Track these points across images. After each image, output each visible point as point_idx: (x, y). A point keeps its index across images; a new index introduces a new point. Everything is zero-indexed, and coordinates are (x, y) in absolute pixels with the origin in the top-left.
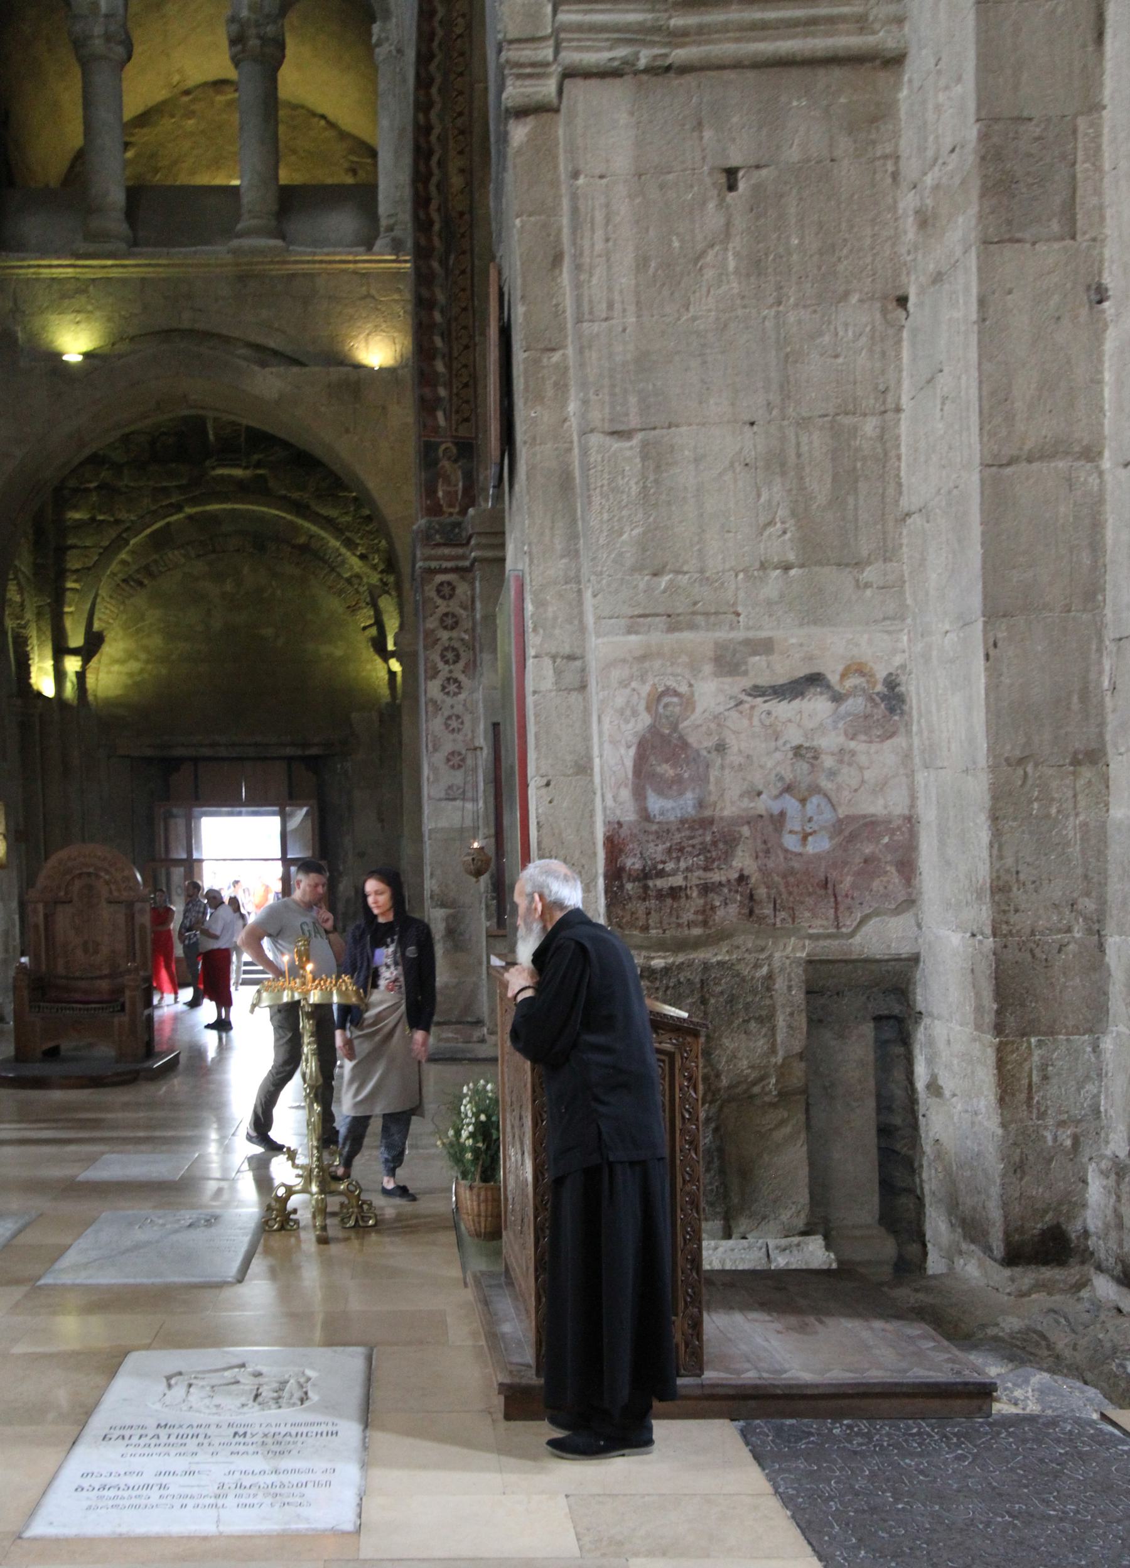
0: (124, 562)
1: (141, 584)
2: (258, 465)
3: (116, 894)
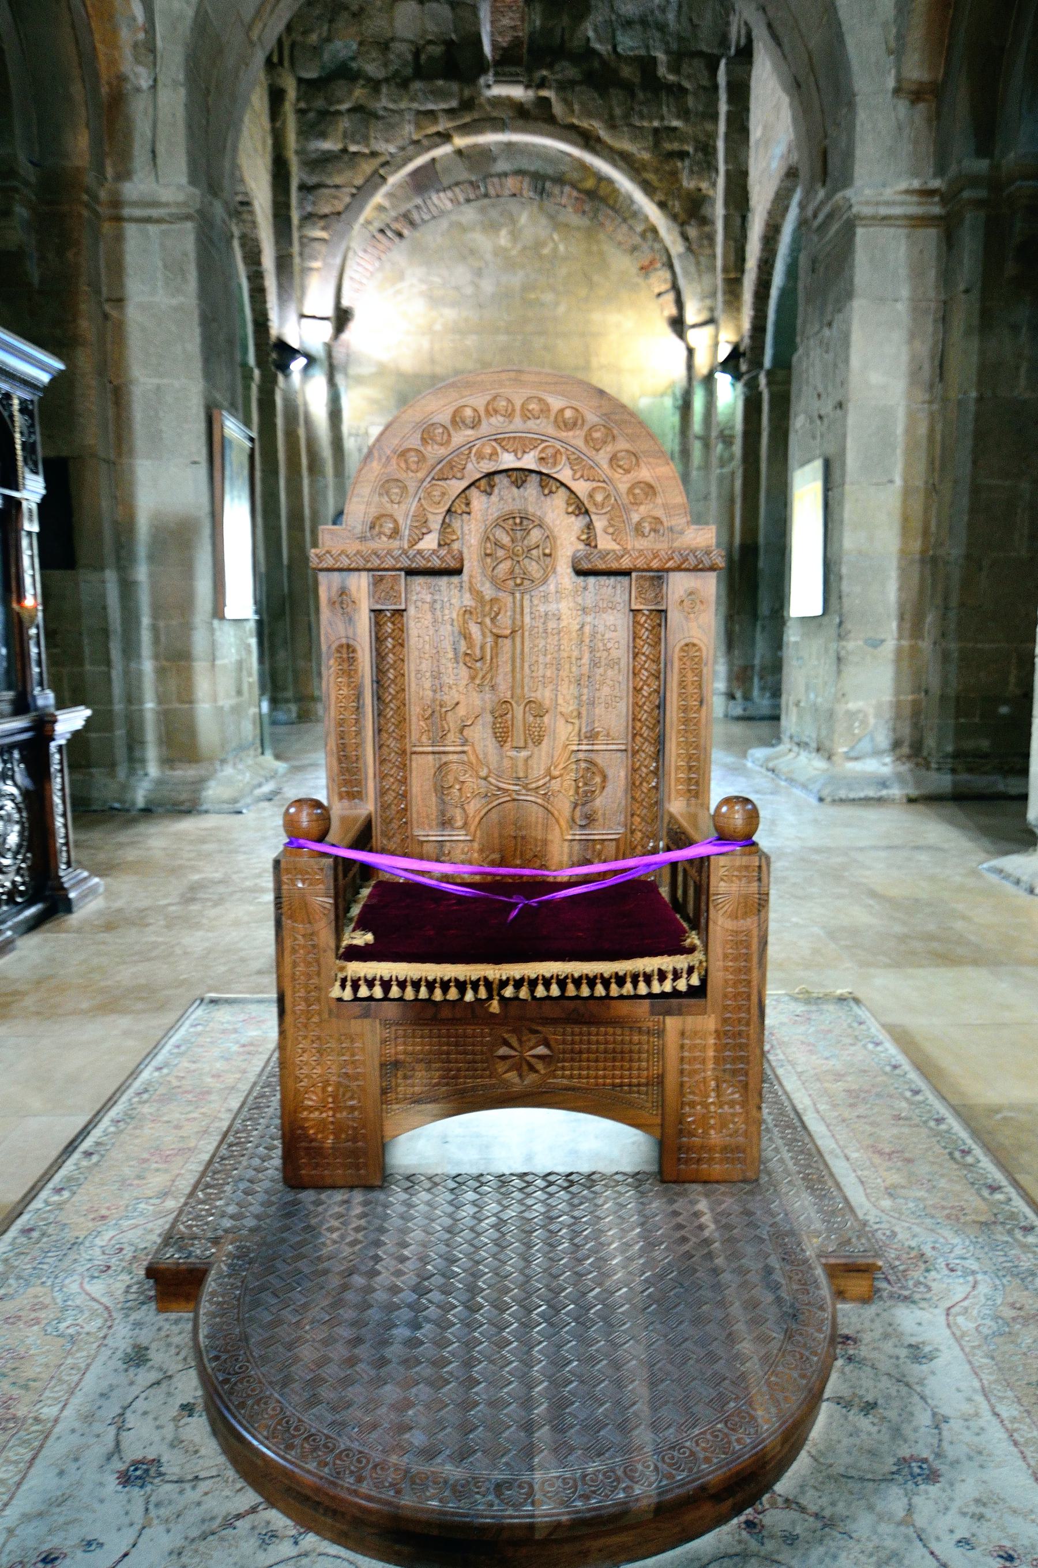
0: (380, 208)
1: (400, 235)
2: (542, 84)
3: (605, 543)
